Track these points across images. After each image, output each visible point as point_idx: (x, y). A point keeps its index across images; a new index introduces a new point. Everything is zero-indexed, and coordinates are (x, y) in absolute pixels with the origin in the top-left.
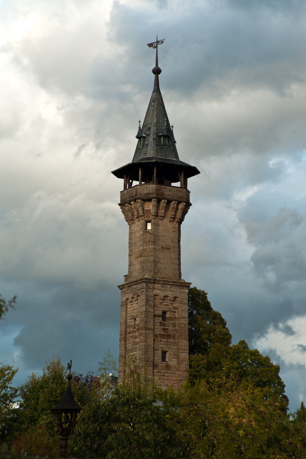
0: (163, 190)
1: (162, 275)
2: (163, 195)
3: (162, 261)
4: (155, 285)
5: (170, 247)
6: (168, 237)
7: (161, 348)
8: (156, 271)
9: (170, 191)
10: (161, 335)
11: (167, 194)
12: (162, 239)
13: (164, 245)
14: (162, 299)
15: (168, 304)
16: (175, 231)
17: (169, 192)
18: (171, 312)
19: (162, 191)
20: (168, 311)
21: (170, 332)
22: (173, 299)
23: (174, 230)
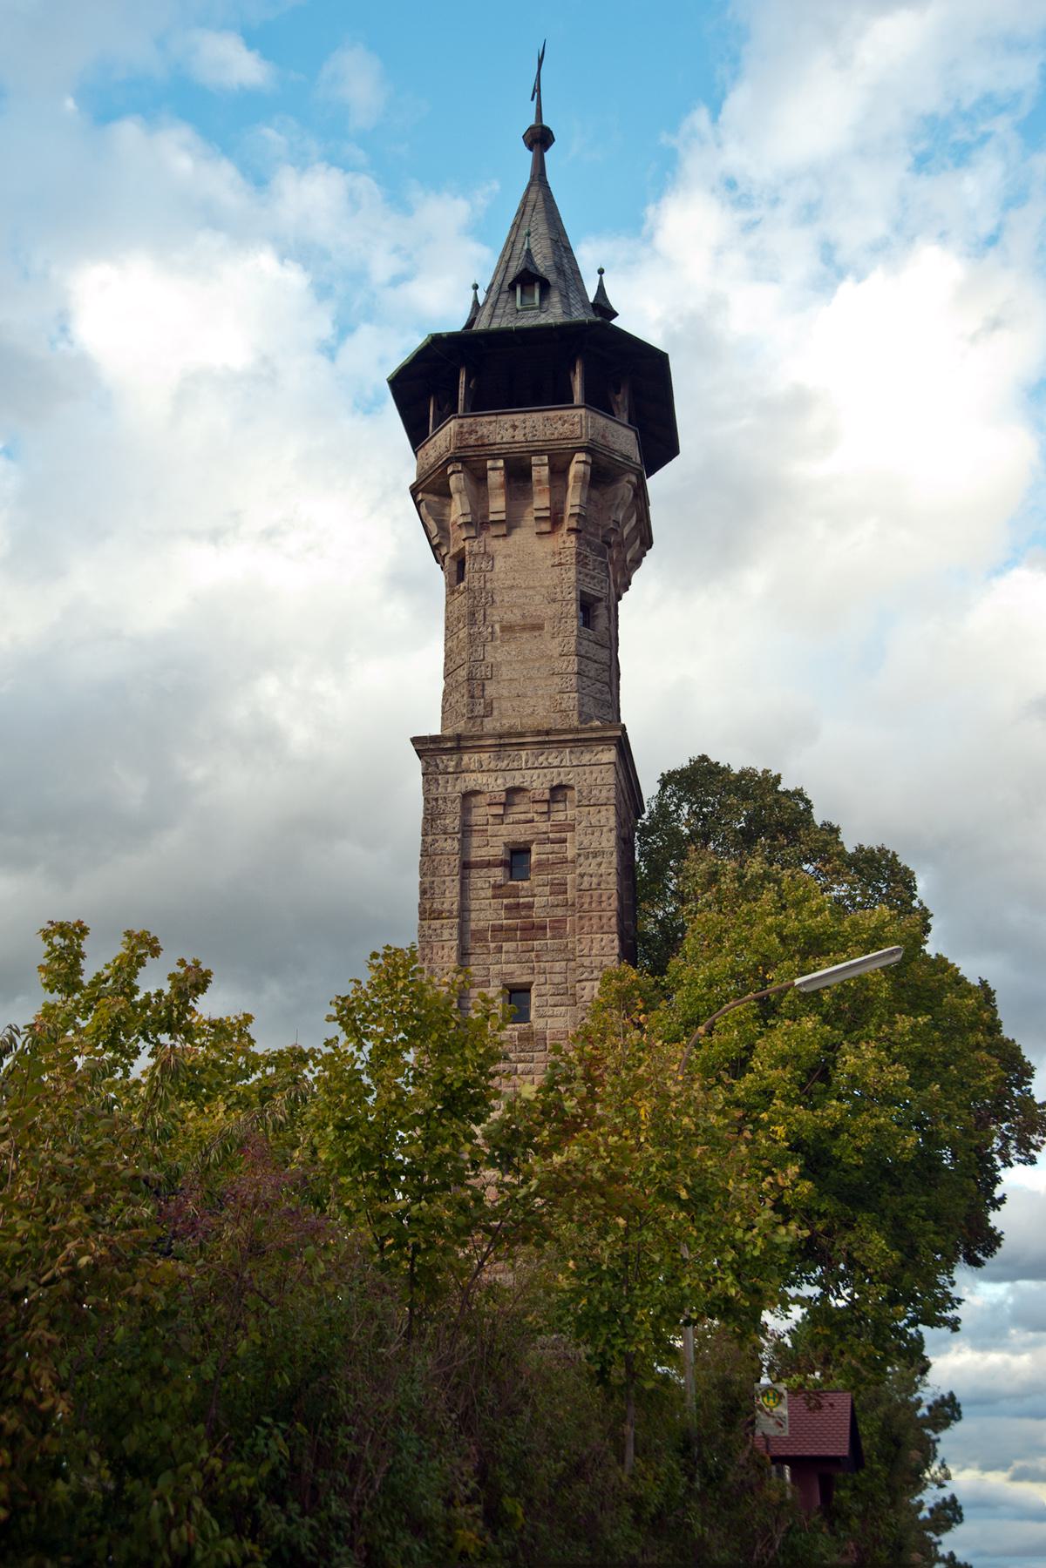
0: (484, 431)
1: (504, 721)
2: (483, 445)
3: (505, 672)
4: (466, 758)
5: (540, 621)
6: (534, 588)
7: (500, 973)
8: (480, 710)
9: (514, 427)
10: (497, 929)
11: (504, 440)
12: (506, 599)
13: (514, 617)
14: (497, 800)
15: (529, 816)
16: (560, 564)
17: (511, 430)
18: (541, 843)
19: (480, 433)
20: (532, 842)
21: (538, 915)
22: (547, 796)
23: (557, 561)
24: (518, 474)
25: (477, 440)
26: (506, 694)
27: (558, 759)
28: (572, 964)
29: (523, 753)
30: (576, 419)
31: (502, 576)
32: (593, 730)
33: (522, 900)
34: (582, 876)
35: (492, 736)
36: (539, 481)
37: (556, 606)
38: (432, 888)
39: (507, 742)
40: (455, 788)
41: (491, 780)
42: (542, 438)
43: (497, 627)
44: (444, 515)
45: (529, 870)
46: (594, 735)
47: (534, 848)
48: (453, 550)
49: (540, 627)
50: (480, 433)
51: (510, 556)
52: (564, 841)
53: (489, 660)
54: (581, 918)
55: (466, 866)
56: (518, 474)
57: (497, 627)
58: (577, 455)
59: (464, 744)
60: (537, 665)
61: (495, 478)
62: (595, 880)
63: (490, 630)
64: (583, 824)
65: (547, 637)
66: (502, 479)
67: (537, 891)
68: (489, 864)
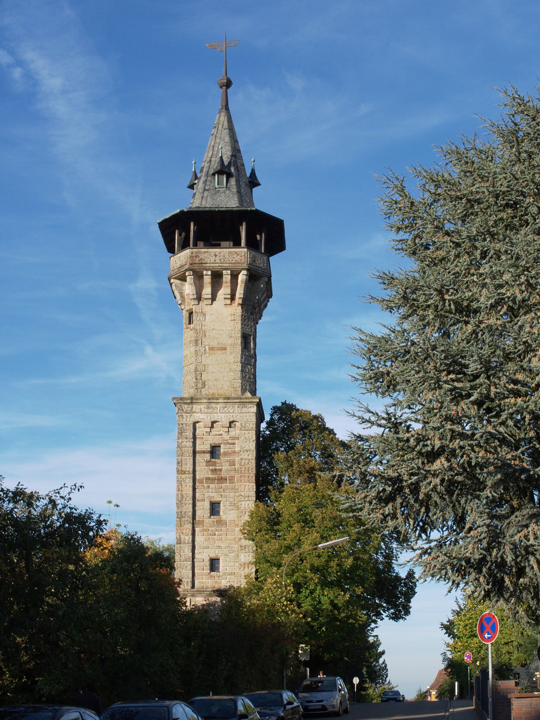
0: (201, 256)
1: (210, 391)
2: (202, 263)
3: (210, 369)
4: (195, 406)
5: (225, 346)
6: (223, 330)
7: (209, 497)
8: (200, 385)
9: (216, 255)
10: (208, 479)
11: (211, 261)
12: (211, 335)
13: (214, 344)
14: (208, 426)
15: (220, 433)
16: (234, 320)
17: (214, 257)
18: (225, 444)
19: (200, 257)
20: (222, 444)
21: (224, 474)
22: (228, 425)
23: (233, 318)
24: (217, 276)
25: (199, 261)
26: (211, 379)
27: (233, 410)
28: (237, 494)
29: (218, 406)
30: (243, 254)
31: (209, 324)
32: (246, 398)
33: (217, 468)
34: (241, 459)
35: (206, 398)
36: (226, 282)
37: (232, 339)
38: (182, 462)
39: (212, 399)
40: (190, 420)
41: (205, 417)
42: (228, 262)
43: (207, 348)
44: (182, 290)
45: (219, 454)
46: (248, 401)
47: (222, 446)
48: (188, 308)
49: (225, 349)
50: (200, 257)
51: (213, 314)
52: (234, 444)
53: (203, 362)
54: (241, 476)
55: (195, 453)
56: (217, 276)
57: (207, 348)
58: (243, 271)
59: (194, 401)
60: (224, 366)
61: (207, 279)
62: (247, 461)
63: (204, 349)
64: (242, 438)
65: (228, 353)
66: (210, 280)
67: (223, 464)
68: (204, 452)
